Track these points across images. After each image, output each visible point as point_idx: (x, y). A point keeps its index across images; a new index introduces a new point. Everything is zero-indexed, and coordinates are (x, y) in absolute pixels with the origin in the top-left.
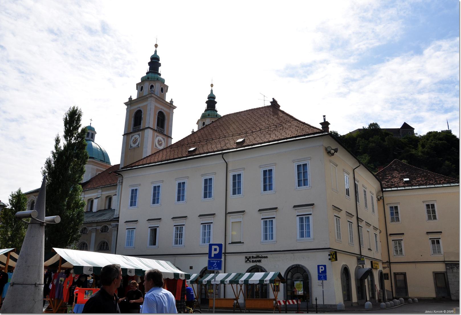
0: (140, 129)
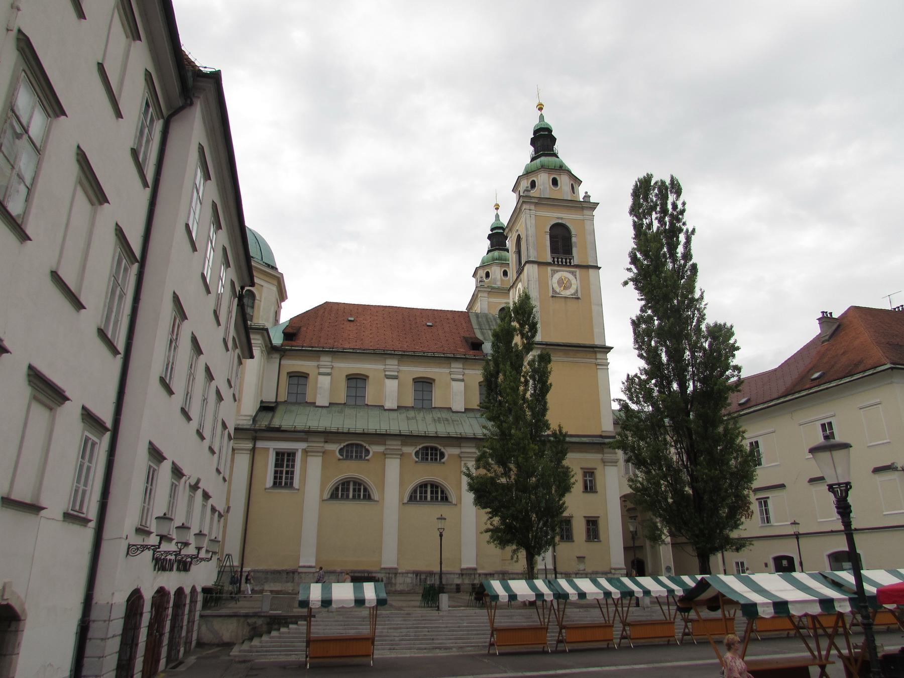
0: (570, 263)
